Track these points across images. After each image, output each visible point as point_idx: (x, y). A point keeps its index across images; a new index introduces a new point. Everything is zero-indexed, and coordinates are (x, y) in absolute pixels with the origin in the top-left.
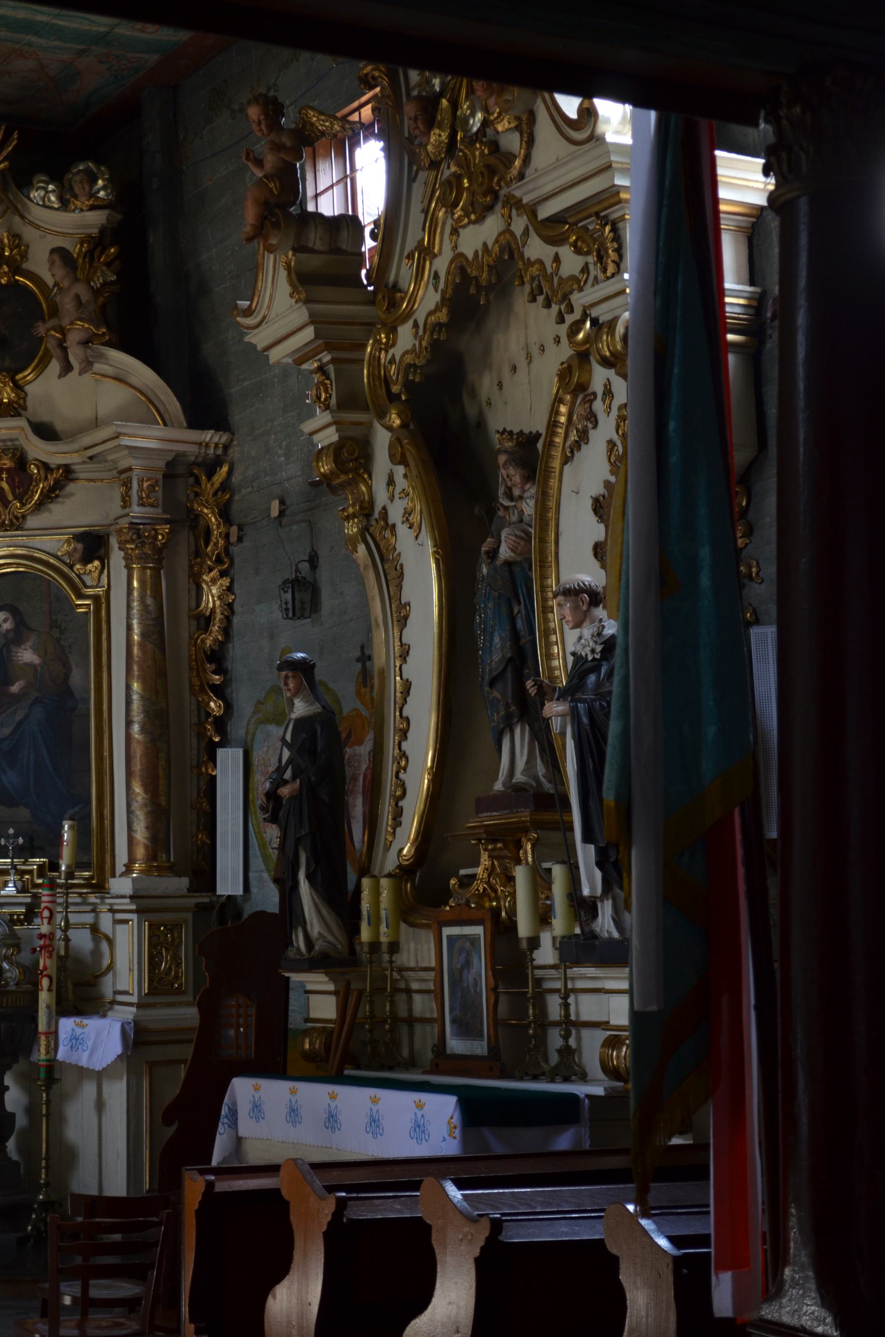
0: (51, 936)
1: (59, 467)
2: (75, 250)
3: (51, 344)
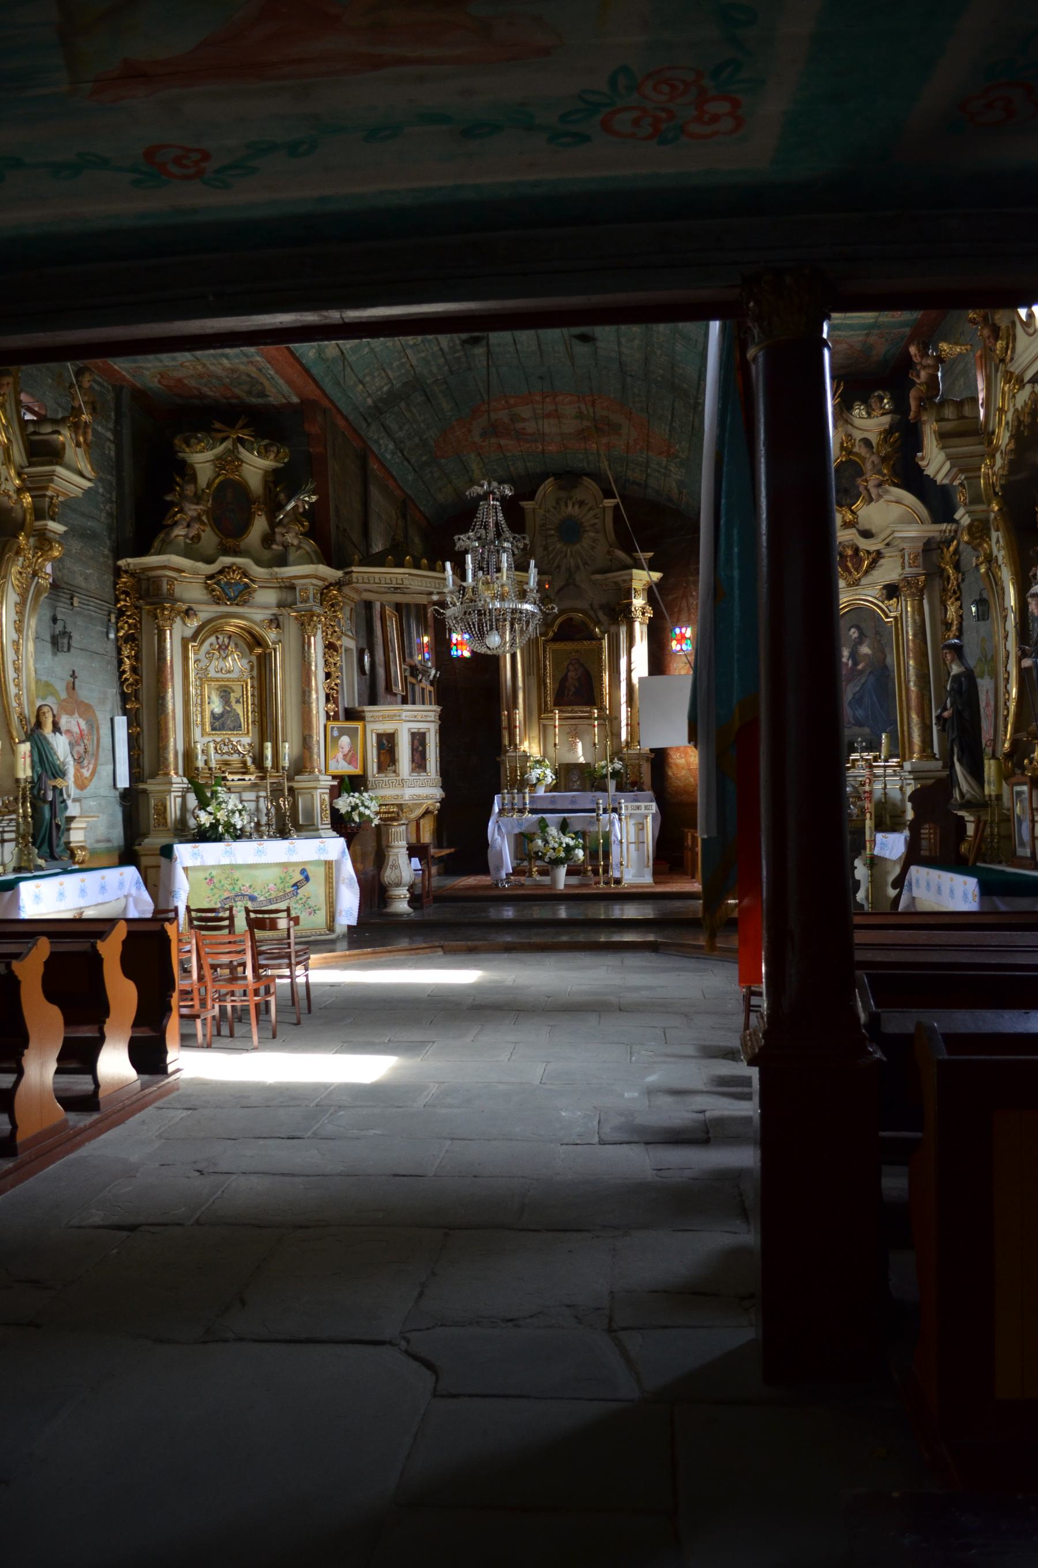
0: (871, 792)
3: (861, 489)
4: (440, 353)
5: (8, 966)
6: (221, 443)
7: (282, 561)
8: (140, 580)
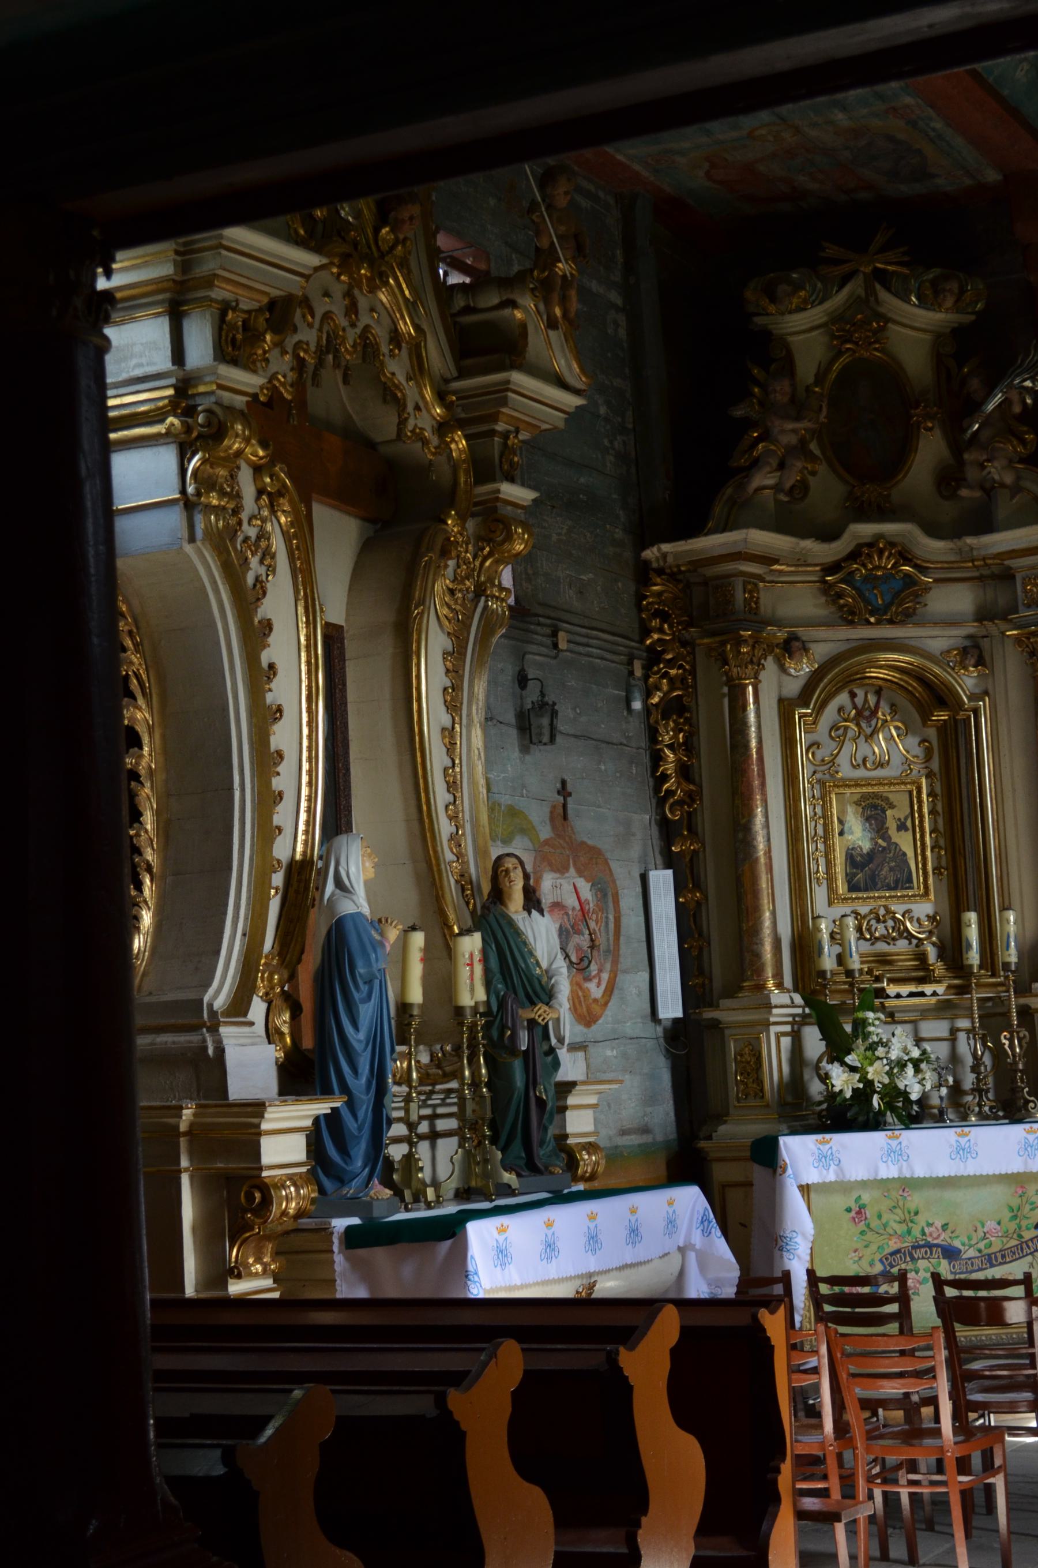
5: (441, 1400)
6: (841, 287)
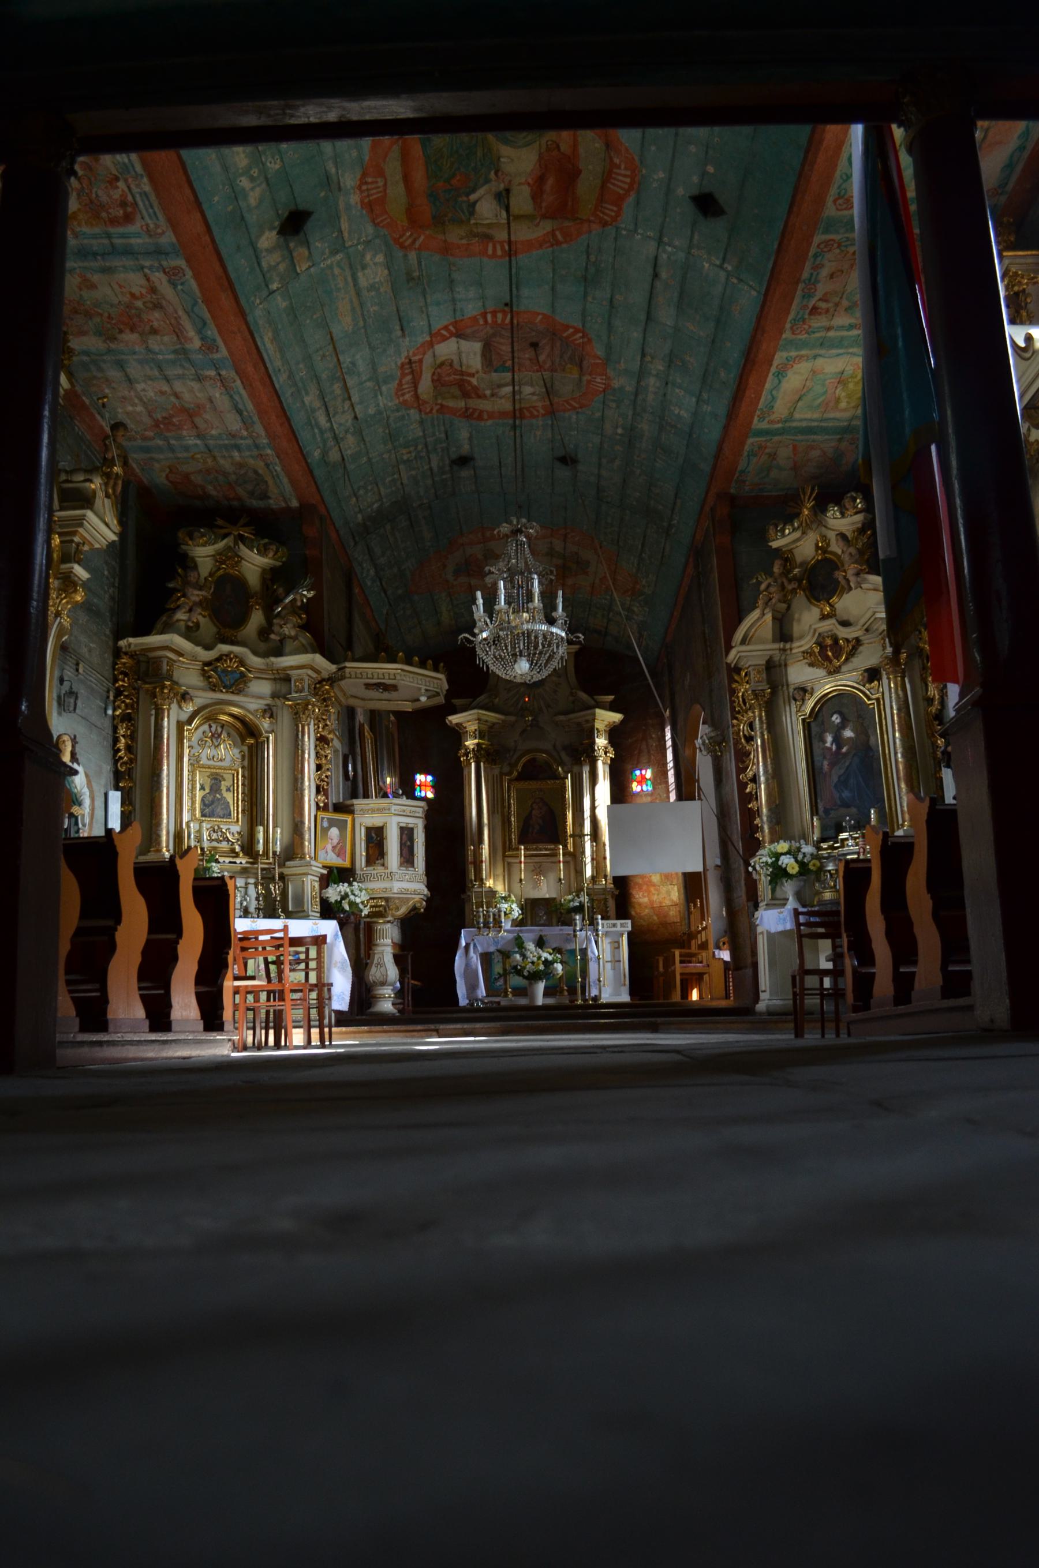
1: (853, 639)
2: (849, 535)
4: (429, 473)
6: (223, 539)
7: (279, 652)
8: (139, 662)
